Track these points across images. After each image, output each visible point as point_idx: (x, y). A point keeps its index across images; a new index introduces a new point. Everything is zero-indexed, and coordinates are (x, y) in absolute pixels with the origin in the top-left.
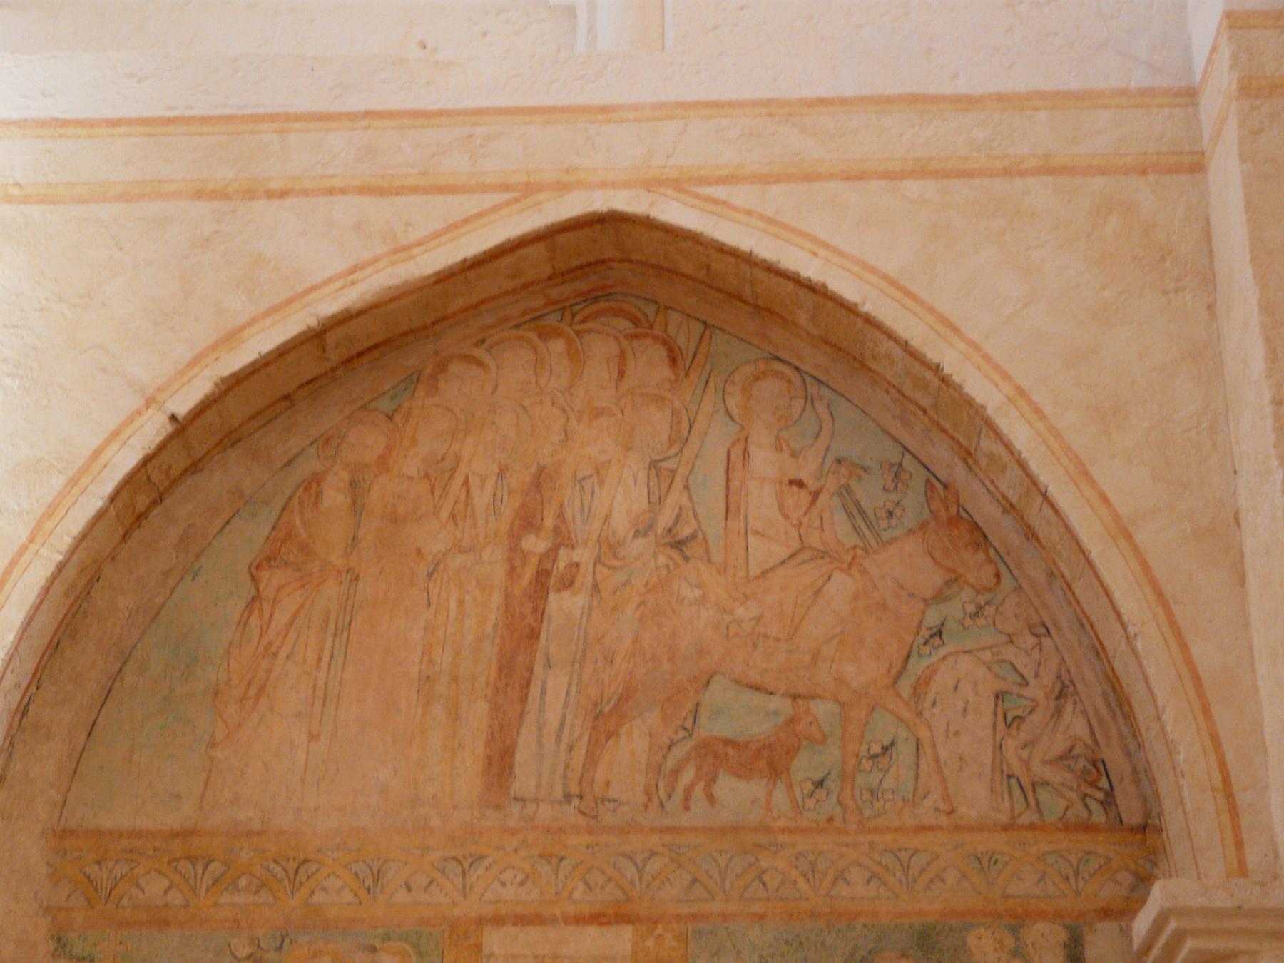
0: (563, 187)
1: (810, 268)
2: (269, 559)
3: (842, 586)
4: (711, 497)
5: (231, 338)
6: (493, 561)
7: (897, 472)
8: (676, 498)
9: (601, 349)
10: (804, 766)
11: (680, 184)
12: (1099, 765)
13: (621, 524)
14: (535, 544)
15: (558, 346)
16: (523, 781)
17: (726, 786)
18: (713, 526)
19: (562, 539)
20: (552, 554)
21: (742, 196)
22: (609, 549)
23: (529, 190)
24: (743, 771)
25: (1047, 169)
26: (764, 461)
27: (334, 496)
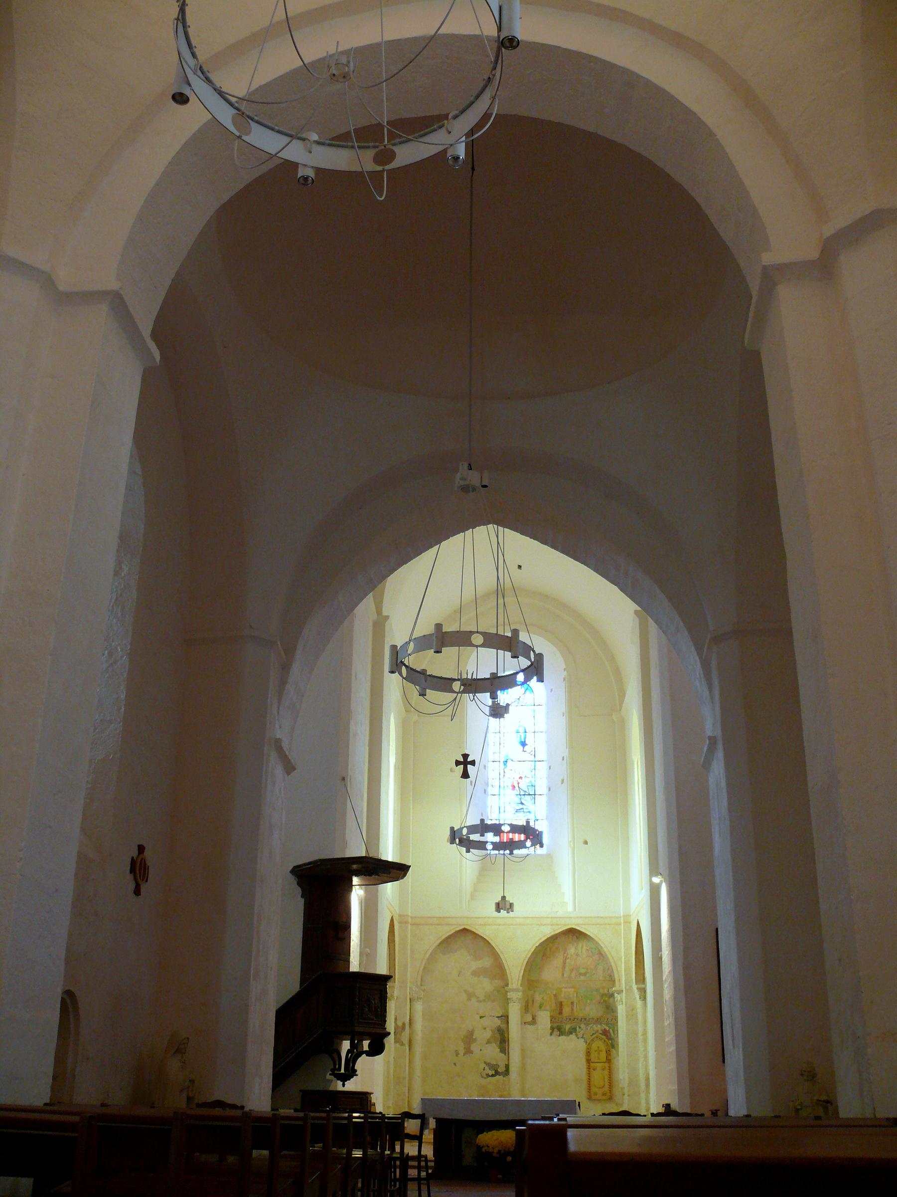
0: (568, 925)
1: (589, 934)
2: (543, 956)
3: (591, 959)
4: (580, 951)
5: (541, 939)
6: (562, 957)
7: (596, 949)
8: (577, 951)
9: (571, 936)
10: (588, 975)
11: (578, 925)
12: (611, 976)
13: (572, 953)
14: (565, 955)
15: (567, 936)
16: (565, 975)
17: (581, 977)
18: (580, 954)
19: (567, 955)
20: (566, 957)
21: (584, 926)
22: (571, 955)
23: (565, 925)
24: (583, 975)
25: (609, 924)
26: (584, 948)
27: (548, 949)
